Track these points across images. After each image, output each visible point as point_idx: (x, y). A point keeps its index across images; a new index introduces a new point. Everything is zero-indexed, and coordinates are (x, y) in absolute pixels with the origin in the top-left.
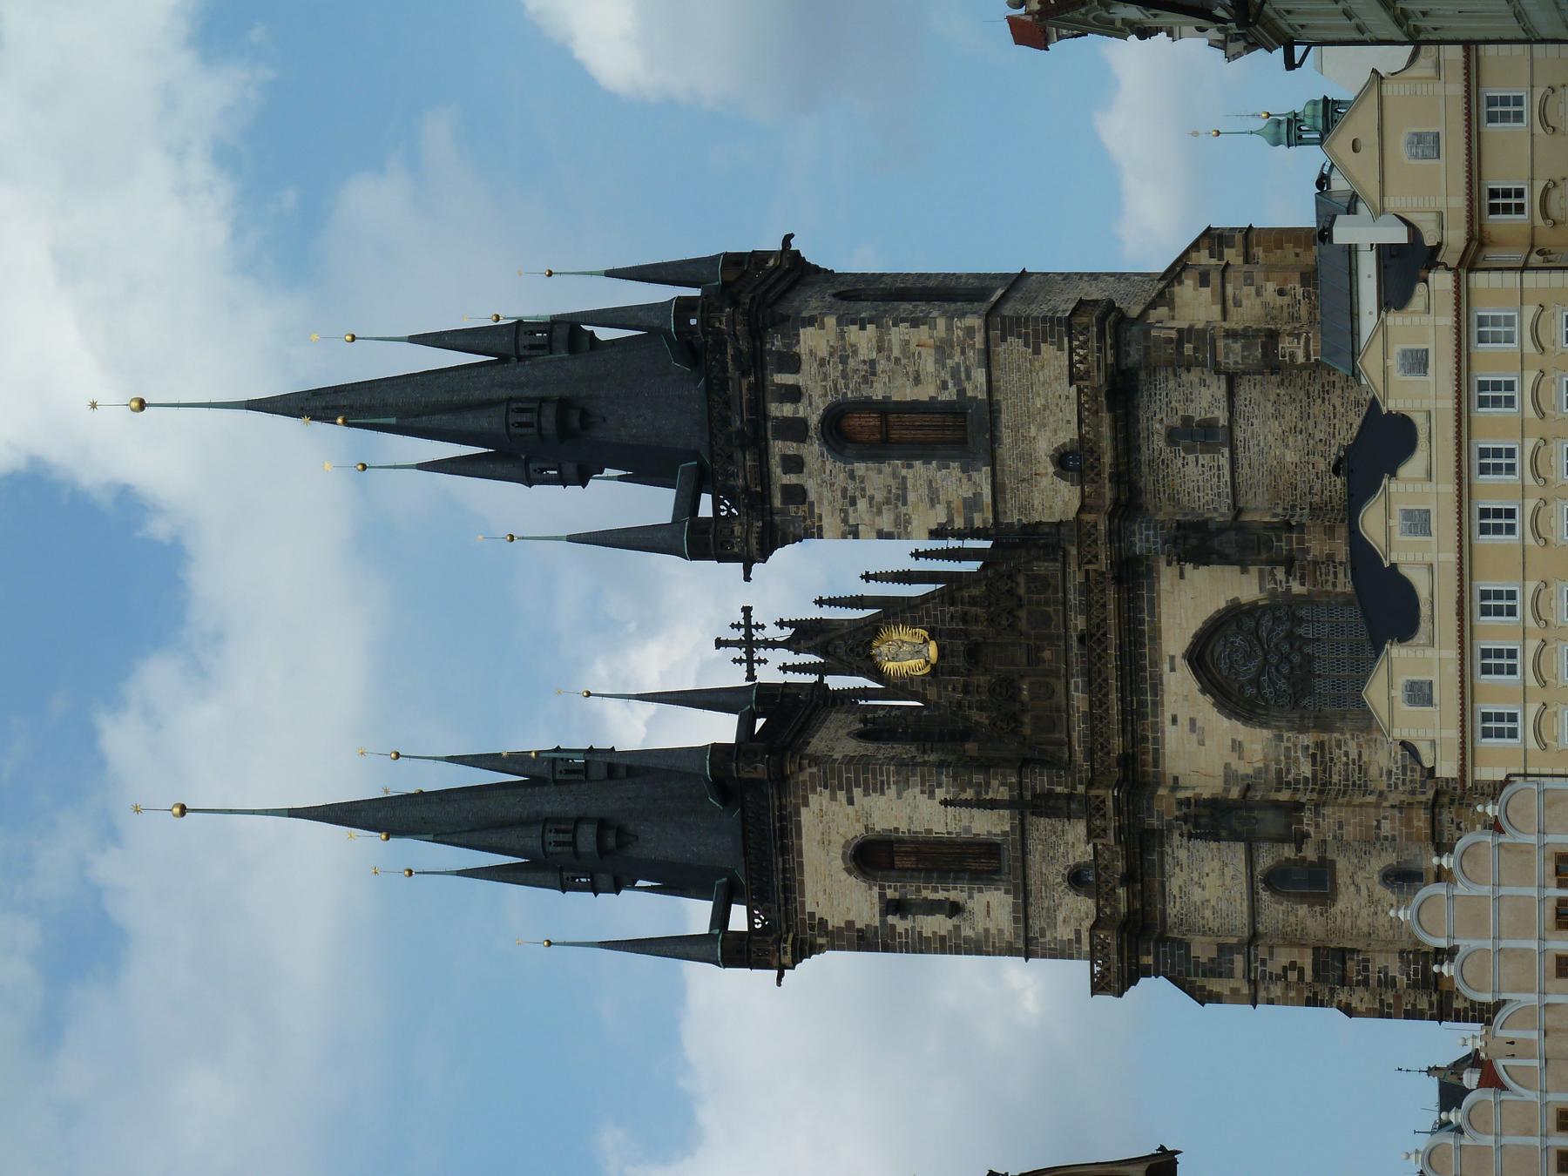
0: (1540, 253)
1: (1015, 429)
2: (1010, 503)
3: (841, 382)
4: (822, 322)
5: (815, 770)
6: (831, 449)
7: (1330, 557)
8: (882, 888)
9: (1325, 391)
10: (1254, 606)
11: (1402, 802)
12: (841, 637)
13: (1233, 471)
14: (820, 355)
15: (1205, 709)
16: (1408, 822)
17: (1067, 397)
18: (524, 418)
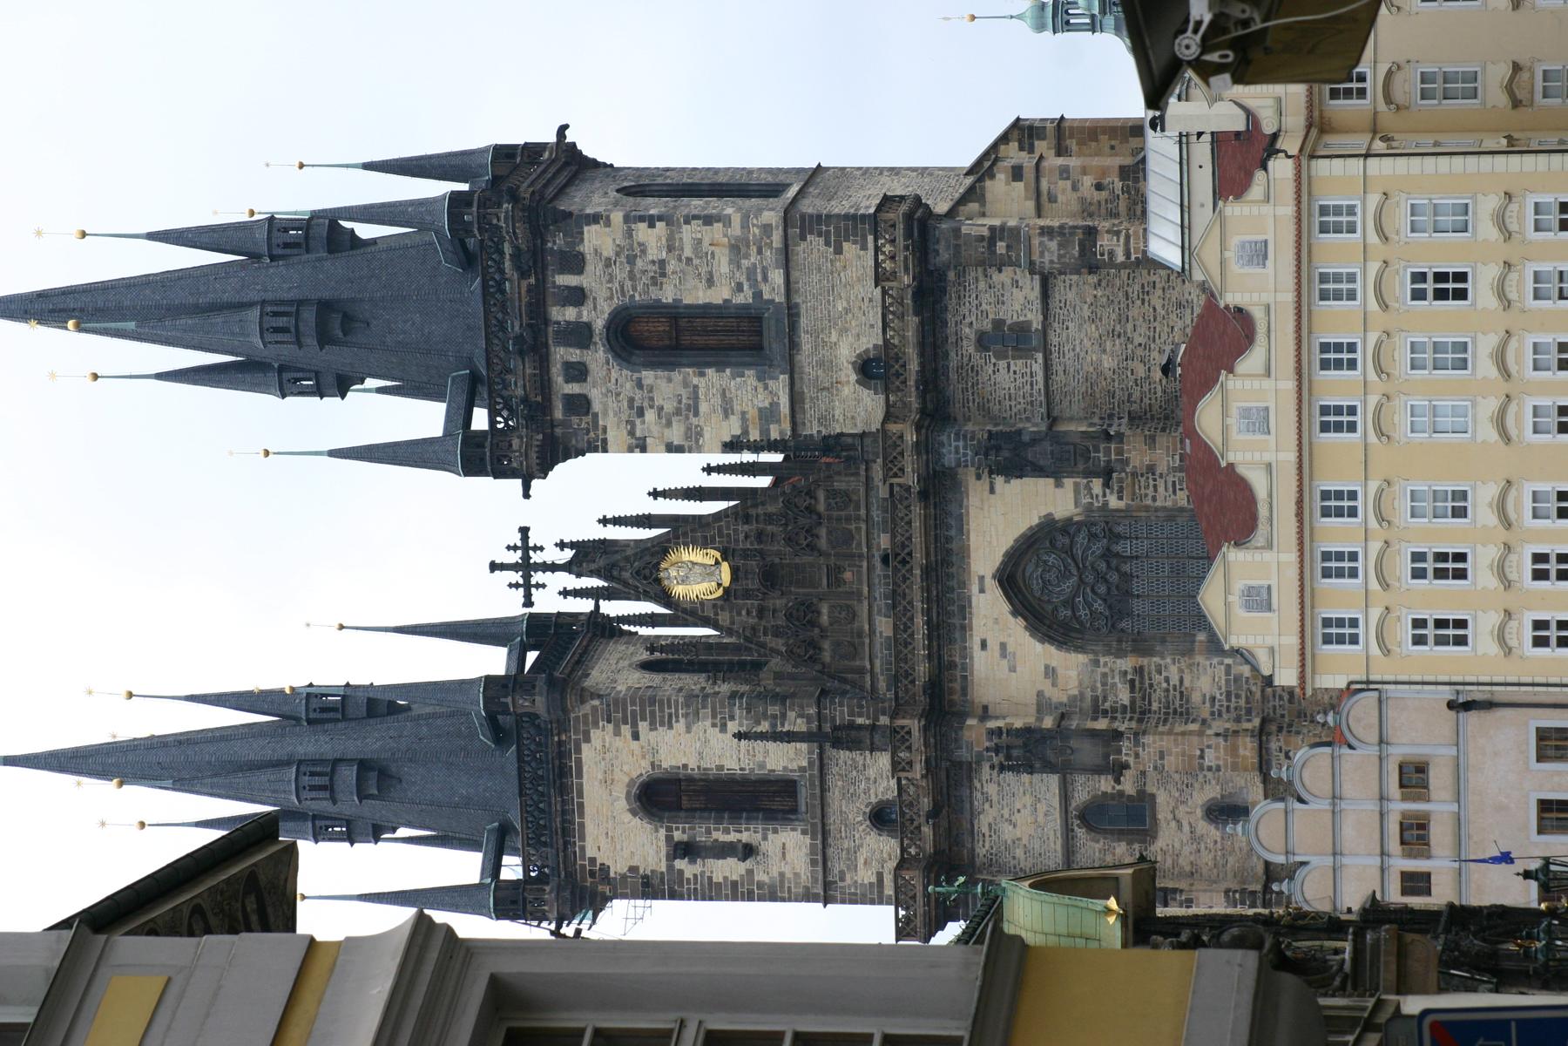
0: (1385, 139)
1: (815, 334)
2: (810, 413)
3: (628, 284)
4: (608, 218)
5: (596, 702)
6: (617, 356)
7: (1151, 469)
8: (669, 829)
9: (1144, 292)
10: (1069, 520)
11: (1227, 730)
12: (627, 559)
13: (1047, 378)
14: (605, 254)
15: (1016, 632)
16: (1234, 751)
17: (871, 300)
18: (281, 322)
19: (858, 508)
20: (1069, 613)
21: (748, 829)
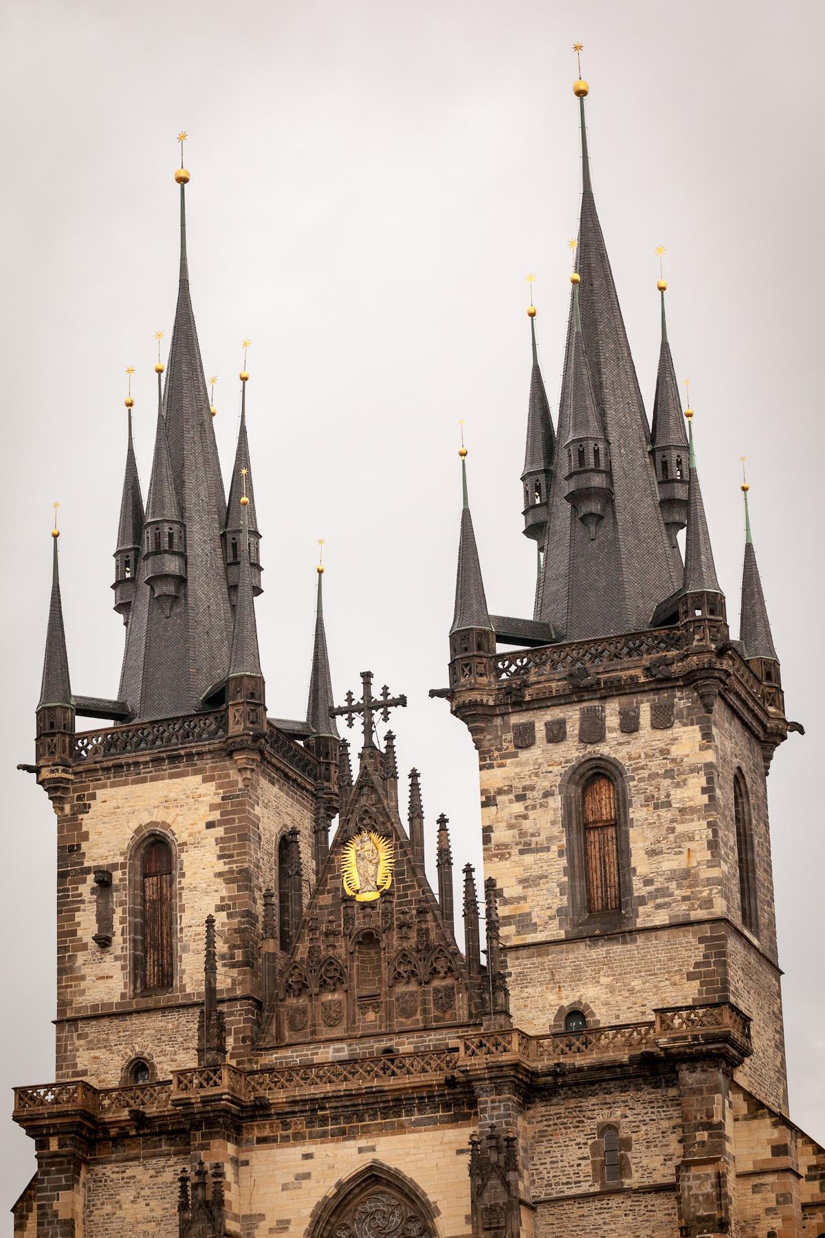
1: (608, 961)
3: (645, 774)
5: (241, 785)
6: (574, 770)
8: (123, 866)
12: (379, 801)
15: (322, 1188)
17: (643, 1013)
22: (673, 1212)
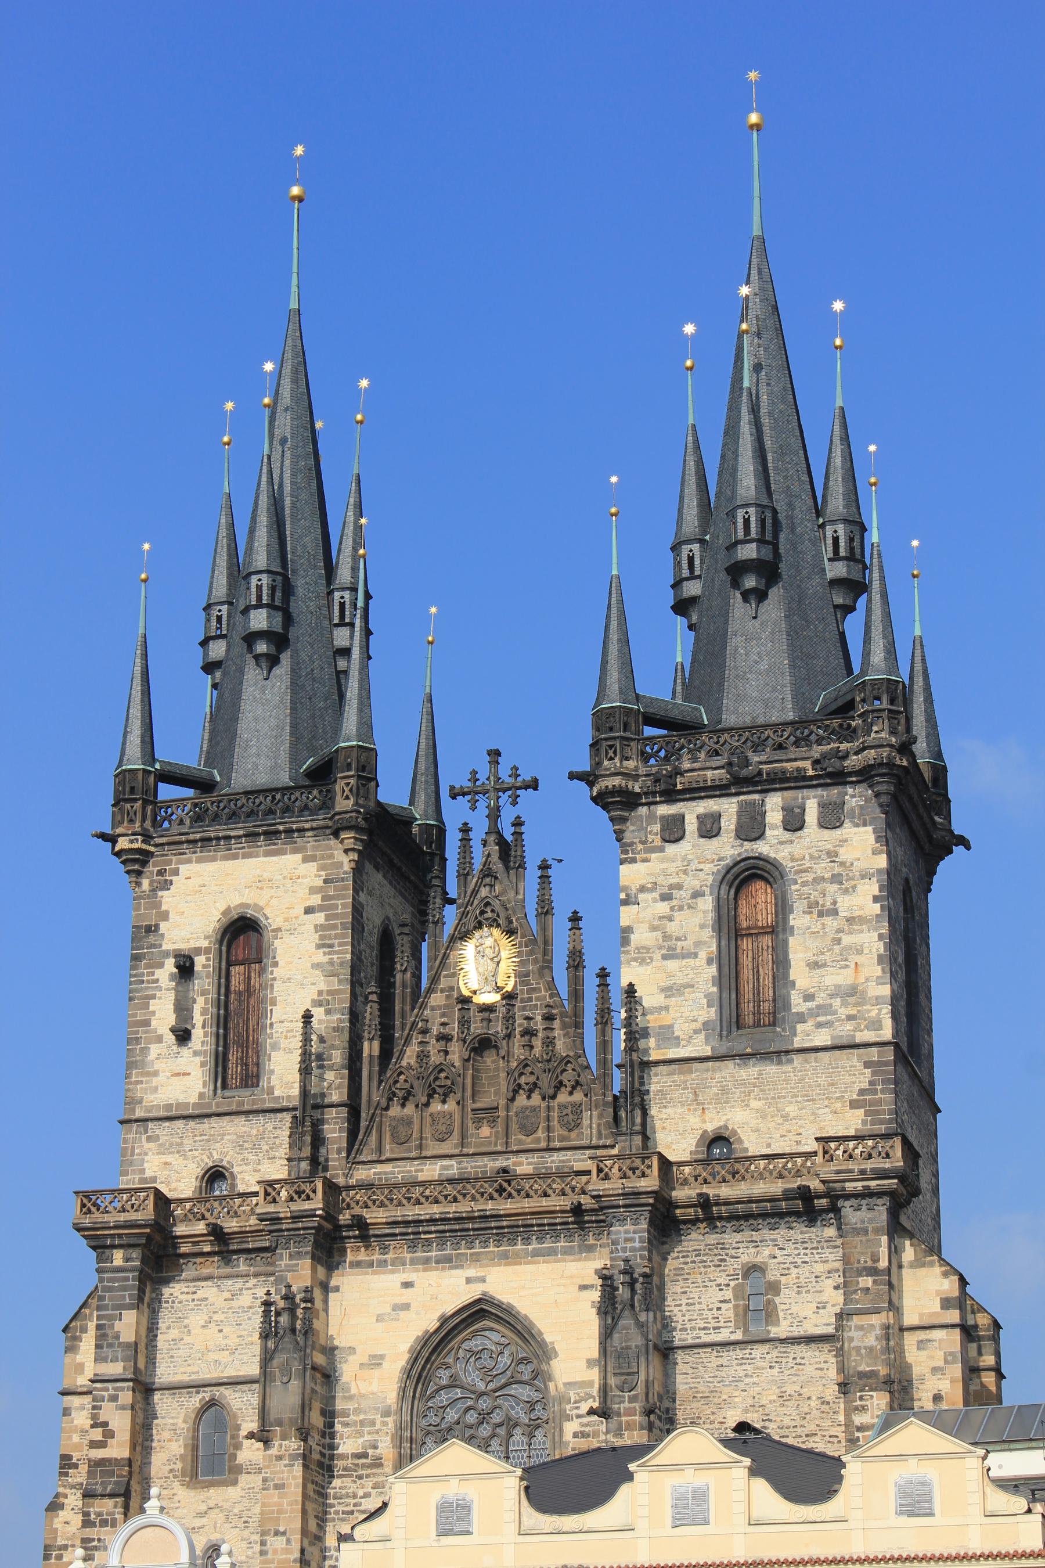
3: (809, 877)
5: (347, 867)
8: (207, 951)
14: (842, 851)
17: (798, 1143)
19: (562, 1139)
20: (444, 1383)
21: (206, 1035)
22: (825, 1366)
